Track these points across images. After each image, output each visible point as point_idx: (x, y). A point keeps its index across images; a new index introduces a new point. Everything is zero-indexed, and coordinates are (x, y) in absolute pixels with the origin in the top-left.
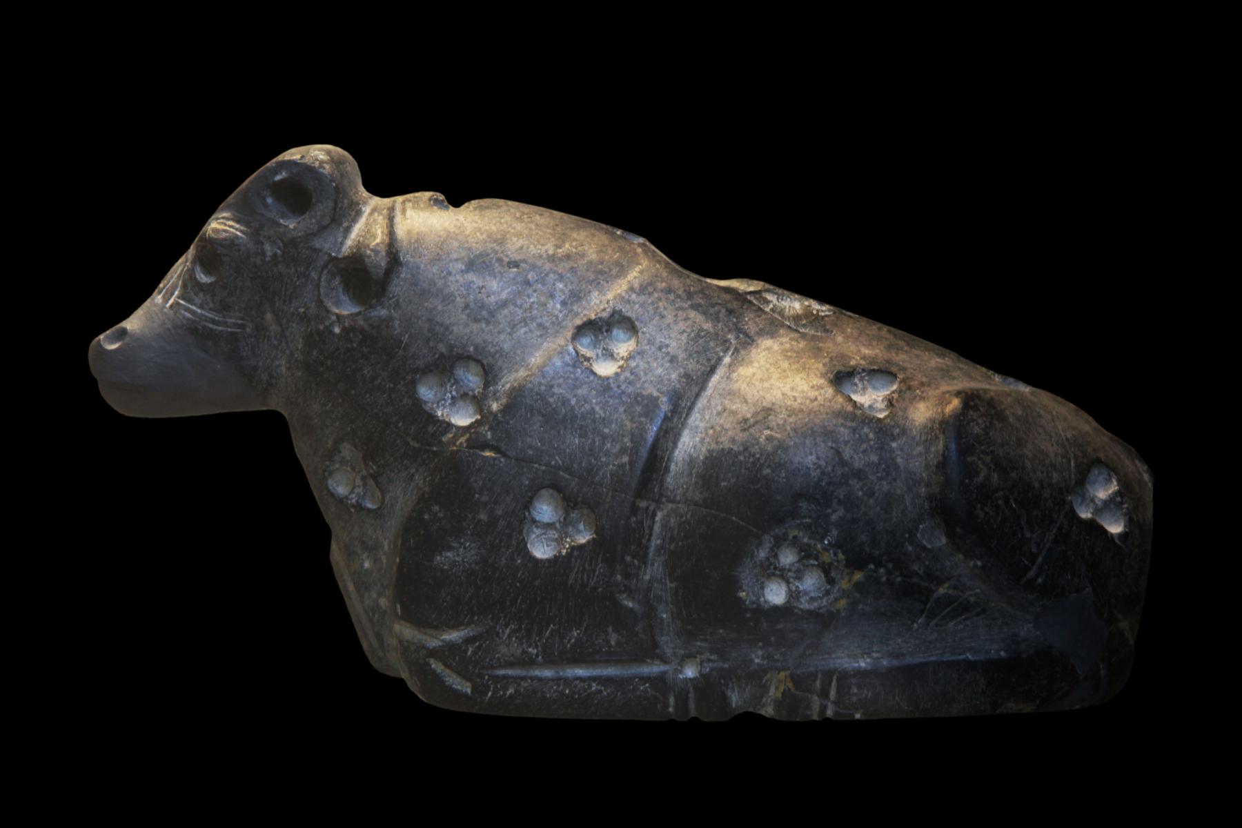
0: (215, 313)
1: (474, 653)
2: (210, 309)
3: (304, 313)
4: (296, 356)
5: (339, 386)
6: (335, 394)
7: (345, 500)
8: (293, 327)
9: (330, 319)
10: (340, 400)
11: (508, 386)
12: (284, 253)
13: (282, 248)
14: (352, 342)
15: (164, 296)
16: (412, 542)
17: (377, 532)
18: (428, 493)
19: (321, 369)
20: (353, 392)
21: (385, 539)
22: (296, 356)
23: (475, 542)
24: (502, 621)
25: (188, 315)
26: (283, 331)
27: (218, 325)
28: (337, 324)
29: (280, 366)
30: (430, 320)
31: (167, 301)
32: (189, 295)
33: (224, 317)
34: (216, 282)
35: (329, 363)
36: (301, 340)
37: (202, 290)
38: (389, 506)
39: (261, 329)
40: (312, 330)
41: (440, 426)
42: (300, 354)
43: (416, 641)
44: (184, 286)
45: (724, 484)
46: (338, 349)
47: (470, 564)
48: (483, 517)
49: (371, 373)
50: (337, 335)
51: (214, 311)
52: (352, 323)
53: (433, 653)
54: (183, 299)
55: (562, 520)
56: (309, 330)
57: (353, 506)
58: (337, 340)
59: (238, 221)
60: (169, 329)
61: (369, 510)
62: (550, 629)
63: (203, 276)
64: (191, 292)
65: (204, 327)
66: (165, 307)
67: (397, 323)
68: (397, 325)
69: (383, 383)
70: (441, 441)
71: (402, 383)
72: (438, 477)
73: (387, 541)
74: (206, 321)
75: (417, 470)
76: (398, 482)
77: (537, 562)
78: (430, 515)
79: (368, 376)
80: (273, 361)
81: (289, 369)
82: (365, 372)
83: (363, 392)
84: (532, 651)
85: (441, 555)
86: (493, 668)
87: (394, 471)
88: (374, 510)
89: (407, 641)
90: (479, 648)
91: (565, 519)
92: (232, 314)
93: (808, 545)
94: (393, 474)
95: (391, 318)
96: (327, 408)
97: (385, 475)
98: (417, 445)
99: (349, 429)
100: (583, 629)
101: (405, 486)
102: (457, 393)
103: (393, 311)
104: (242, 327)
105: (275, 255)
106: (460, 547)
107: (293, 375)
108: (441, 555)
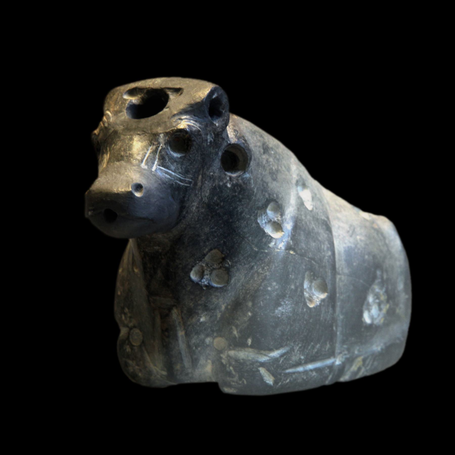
0: (181, 175)
1: (283, 361)
2: (180, 173)
3: (212, 175)
4: (204, 200)
5: (224, 217)
6: (221, 222)
7: (200, 283)
8: (206, 183)
9: (226, 178)
10: (222, 226)
11: (289, 216)
12: (214, 140)
13: (214, 137)
14: (235, 192)
15: (147, 164)
16: (262, 303)
17: (220, 300)
18: (269, 276)
19: (217, 208)
20: (231, 220)
21: (224, 303)
22: (204, 200)
23: (290, 301)
24: (297, 343)
25: (169, 177)
26: (202, 186)
27: (182, 182)
28: (229, 182)
29: (193, 206)
30: (262, 180)
31: (152, 167)
32: (167, 164)
33: (185, 178)
34: (185, 157)
35: (222, 204)
36: (208, 191)
37: (175, 161)
38: (233, 285)
39: (196, 184)
40: (216, 185)
41: (268, 239)
42: (206, 199)
43: (250, 358)
44: (162, 158)
45: (355, 264)
46: (228, 196)
47: (288, 313)
48: (293, 287)
49: (241, 209)
50: (229, 188)
51: (181, 174)
52: (237, 181)
53: (263, 365)
54: (162, 166)
55: (309, 286)
56: (214, 185)
57: (206, 286)
58: (228, 191)
59: (196, 121)
60: (160, 184)
61: (217, 288)
62: (311, 345)
63: (172, 153)
64: (169, 162)
65: (176, 183)
66: (152, 171)
67: (252, 181)
68: (252, 183)
69: (245, 215)
70: (269, 247)
71: (253, 215)
72: (274, 266)
73: (225, 304)
74: (177, 180)
75: (256, 263)
76: (242, 270)
77: (310, 309)
78: (271, 287)
79: (240, 211)
80: (192, 203)
81: (197, 208)
82: (239, 209)
83: (235, 220)
84: (302, 357)
85: (277, 309)
86: (287, 369)
87: (241, 265)
88: (221, 288)
89: (243, 359)
90: (285, 359)
91: (310, 286)
92: (188, 176)
93: (378, 293)
94: (241, 266)
95: (250, 179)
96: (214, 229)
97: (235, 267)
98: (256, 250)
99: (222, 242)
100: (321, 343)
101: (247, 273)
102: (267, 220)
103: (251, 175)
104: (190, 183)
105: (211, 142)
106: (284, 304)
107: (198, 211)
108: (277, 309)
